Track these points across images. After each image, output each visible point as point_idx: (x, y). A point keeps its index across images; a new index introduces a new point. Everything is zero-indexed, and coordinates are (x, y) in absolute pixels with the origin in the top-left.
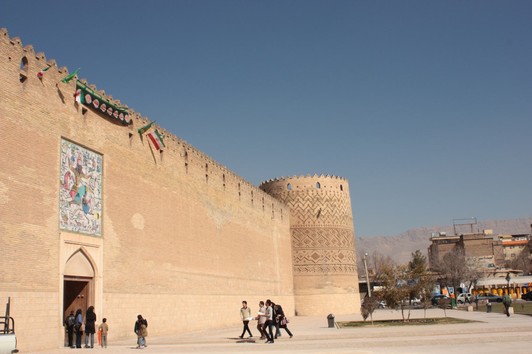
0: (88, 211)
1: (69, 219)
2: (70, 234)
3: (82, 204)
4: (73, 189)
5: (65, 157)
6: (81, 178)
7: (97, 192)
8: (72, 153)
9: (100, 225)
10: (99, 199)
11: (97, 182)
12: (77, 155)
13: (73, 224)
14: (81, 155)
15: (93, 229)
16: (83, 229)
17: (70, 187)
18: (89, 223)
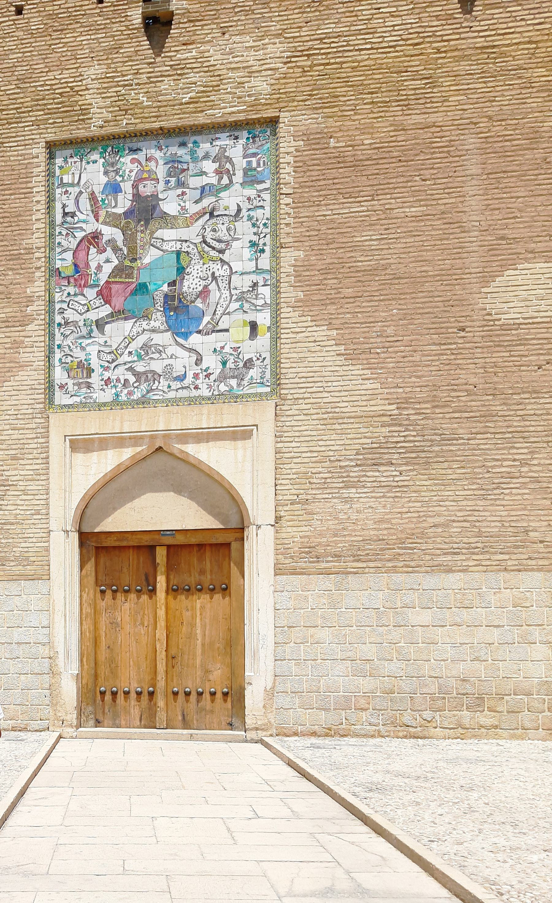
0: (199, 325)
1: (98, 371)
2: (106, 413)
3: (164, 311)
4: (115, 277)
5: (72, 197)
6: (152, 233)
7: (247, 253)
8: (106, 173)
9: (267, 355)
10: (258, 271)
11: (245, 219)
12: (131, 171)
13: (118, 380)
14: (152, 164)
15: (222, 378)
16: (169, 387)
17: (100, 276)
18: (198, 362)
